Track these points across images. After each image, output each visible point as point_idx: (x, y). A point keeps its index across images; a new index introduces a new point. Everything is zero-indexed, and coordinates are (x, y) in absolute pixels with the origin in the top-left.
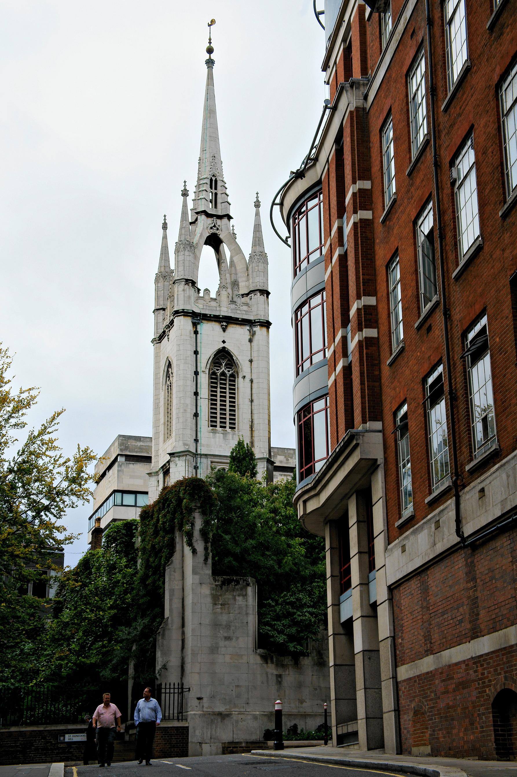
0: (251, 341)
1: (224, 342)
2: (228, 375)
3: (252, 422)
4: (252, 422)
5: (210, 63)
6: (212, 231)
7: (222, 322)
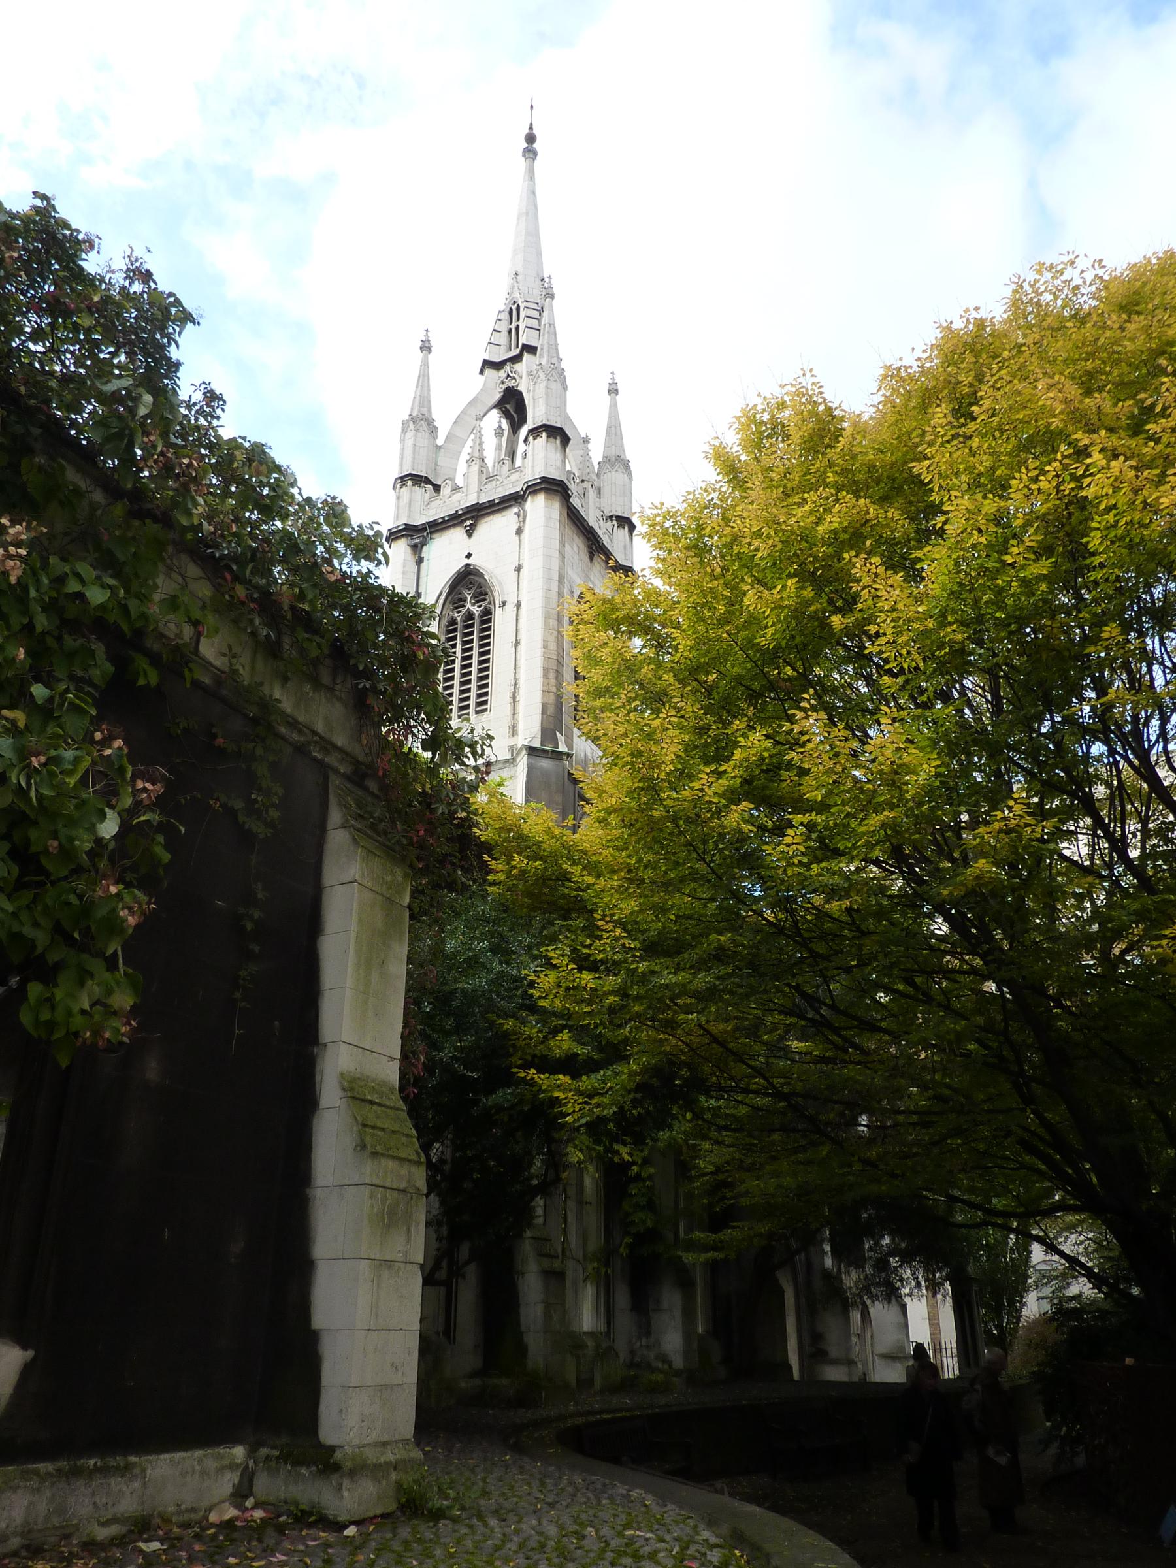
0: (519, 532)
1: (469, 556)
2: (477, 614)
3: (516, 684)
4: (516, 684)
5: (530, 152)
6: (504, 386)
7: (465, 521)
